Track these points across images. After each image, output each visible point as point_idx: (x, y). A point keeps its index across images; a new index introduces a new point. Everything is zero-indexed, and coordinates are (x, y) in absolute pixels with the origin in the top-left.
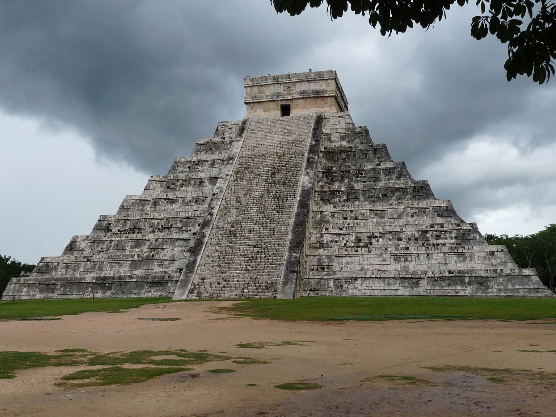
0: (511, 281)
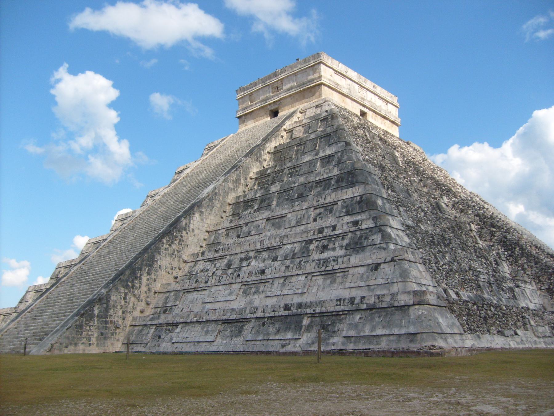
0: (372, 319)
